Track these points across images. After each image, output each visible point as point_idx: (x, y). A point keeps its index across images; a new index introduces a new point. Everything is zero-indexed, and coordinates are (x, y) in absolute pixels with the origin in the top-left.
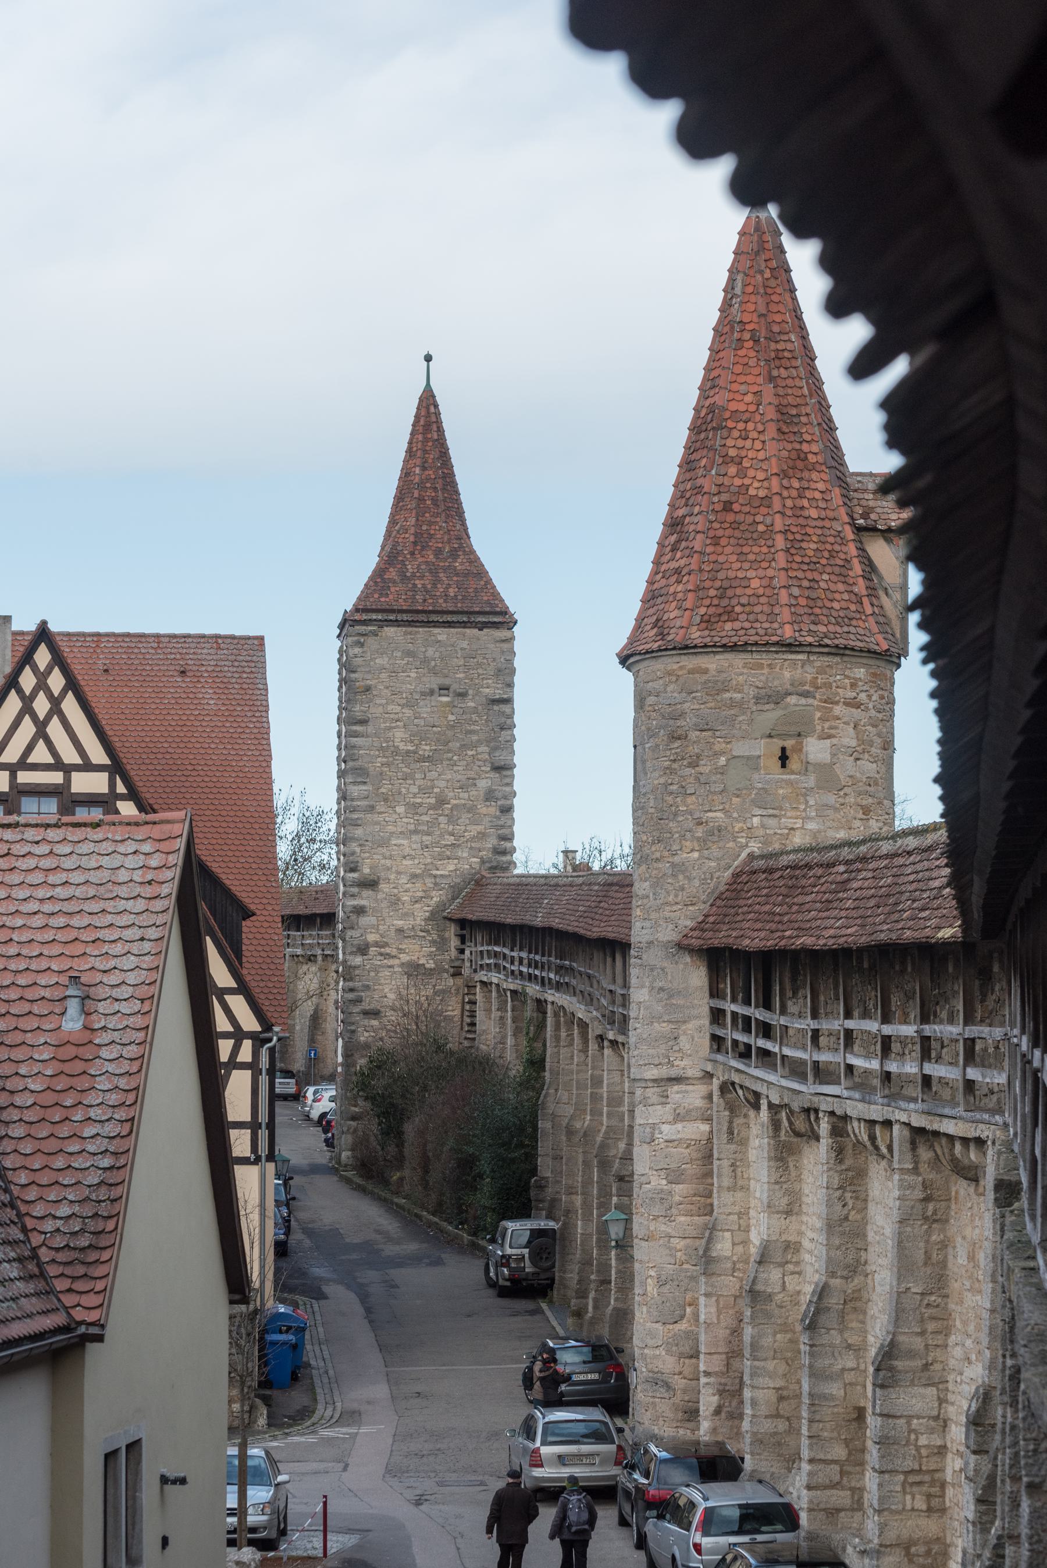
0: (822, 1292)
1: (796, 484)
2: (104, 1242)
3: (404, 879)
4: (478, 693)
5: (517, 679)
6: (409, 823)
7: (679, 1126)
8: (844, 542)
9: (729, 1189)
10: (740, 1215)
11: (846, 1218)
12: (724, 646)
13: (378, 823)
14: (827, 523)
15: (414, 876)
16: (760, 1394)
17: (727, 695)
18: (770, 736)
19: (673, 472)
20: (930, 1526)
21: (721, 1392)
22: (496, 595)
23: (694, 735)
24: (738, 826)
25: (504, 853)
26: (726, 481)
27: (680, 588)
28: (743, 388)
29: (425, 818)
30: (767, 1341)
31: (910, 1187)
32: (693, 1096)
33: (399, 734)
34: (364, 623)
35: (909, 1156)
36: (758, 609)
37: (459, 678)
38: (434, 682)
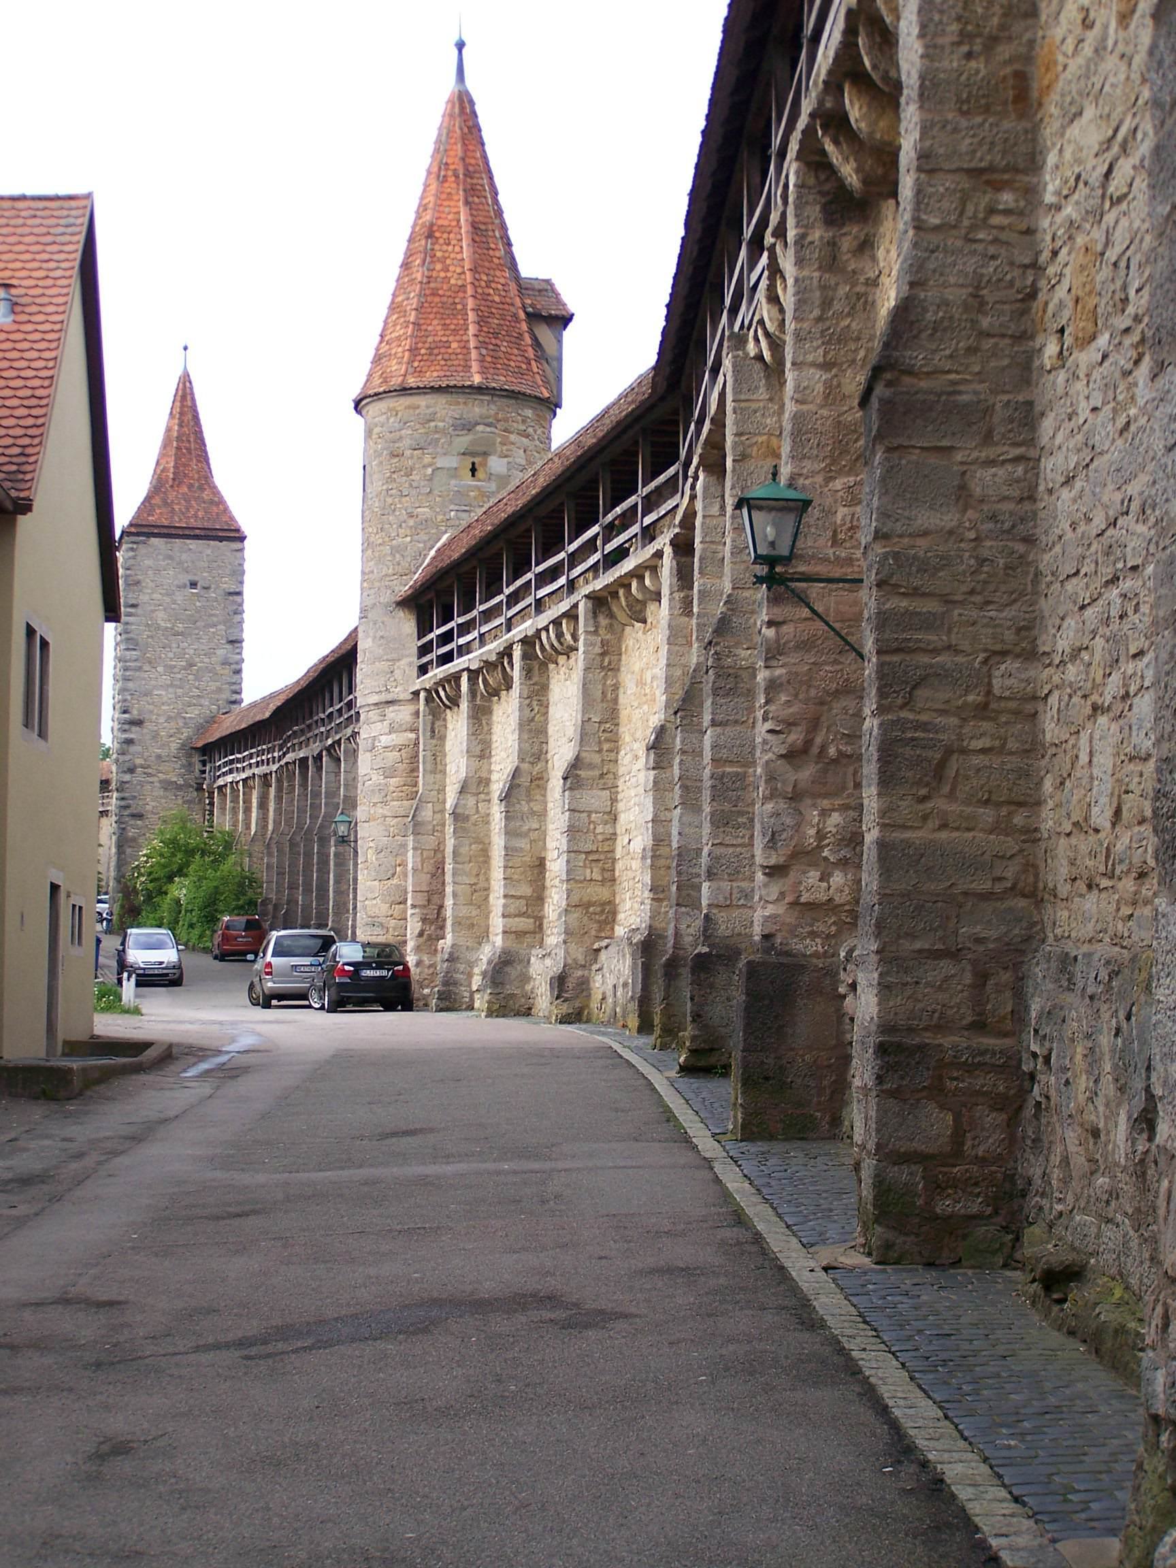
0: (516, 773)
1: (485, 278)
2: (30, 451)
3: (162, 720)
4: (218, 587)
5: (246, 578)
6: (165, 679)
7: (394, 736)
8: (518, 321)
9: (431, 772)
10: (439, 791)
11: (533, 720)
12: (432, 388)
13: (144, 679)
14: (506, 307)
15: (170, 718)
16: (459, 888)
17: (433, 424)
18: (464, 454)
19: (396, 271)
20: (603, 893)
21: (424, 920)
22: (232, 518)
23: (408, 453)
24: (440, 518)
25: (234, 702)
26: (434, 274)
27: (400, 349)
28: (447, 210)
29: (179, 676)
30: (464, 850)
31: (592, 644)
32: (403, 714)
33: (161, 615)
34: (138, 534)
35: (592, 622)
36: (455, 363)
37: (203, 577)
38: (186, 579)
